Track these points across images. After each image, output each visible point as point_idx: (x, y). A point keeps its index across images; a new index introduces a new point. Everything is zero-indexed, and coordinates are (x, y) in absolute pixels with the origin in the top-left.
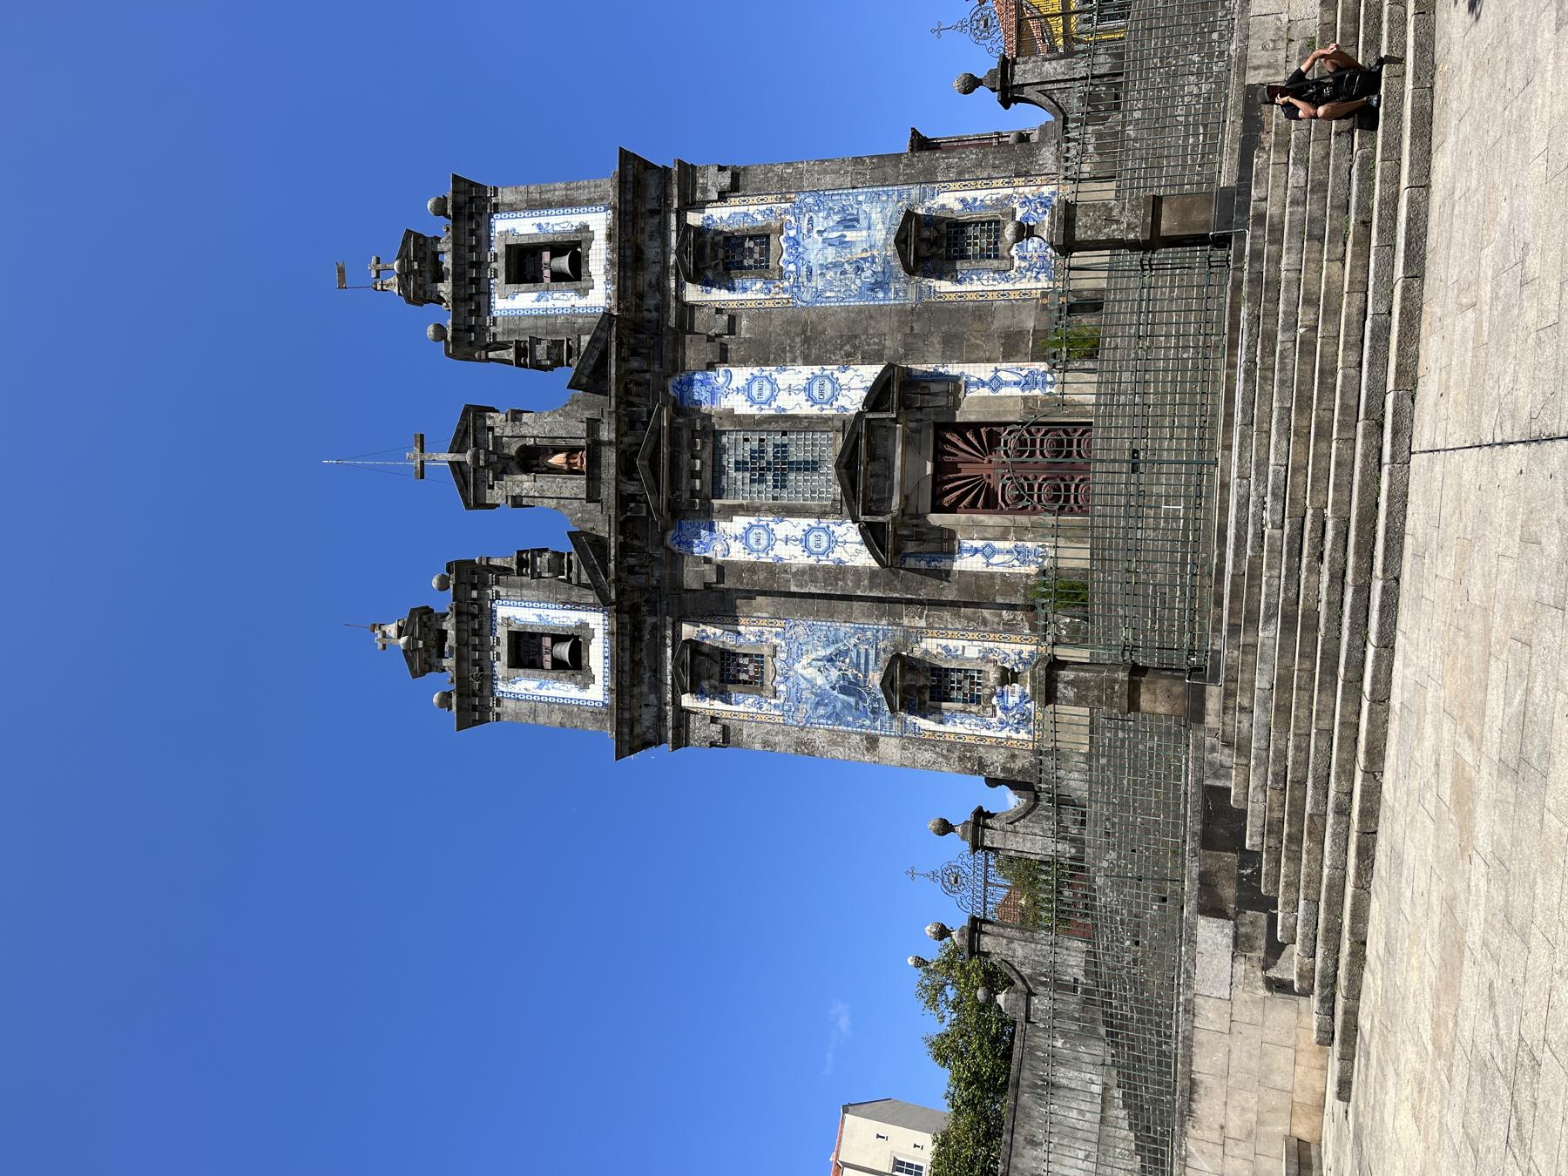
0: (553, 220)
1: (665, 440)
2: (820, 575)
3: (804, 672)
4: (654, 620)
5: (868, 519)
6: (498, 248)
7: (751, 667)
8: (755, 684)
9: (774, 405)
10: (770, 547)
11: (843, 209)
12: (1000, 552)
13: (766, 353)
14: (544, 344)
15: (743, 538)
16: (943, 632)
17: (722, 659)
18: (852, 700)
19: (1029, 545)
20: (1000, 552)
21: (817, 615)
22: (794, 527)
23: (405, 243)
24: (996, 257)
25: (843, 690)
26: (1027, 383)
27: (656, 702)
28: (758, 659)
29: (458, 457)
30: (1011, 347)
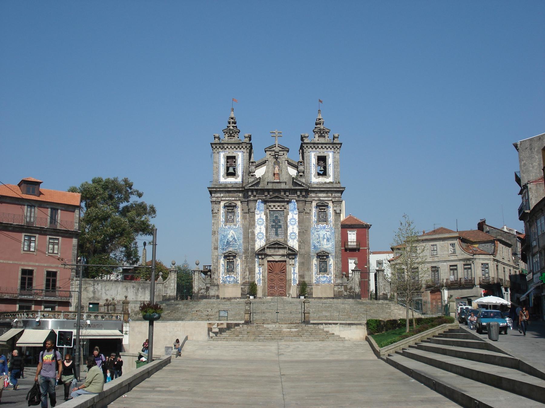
0: (331, 168)
1: (282, 200)
2: (253, 236)
3: (231, 232)
4: (241, 196)
5: (266, 248)
6: (325, 154)
7: (231, 219)
8: (227, 221)
9: (290, 225)
10: (259, 224)
11: (331, 239)
12: (260, 276)
13: (301, 222)
14: (303, 169)
15: (260, 218)
16: (242, 264)
17: (232, 212)
18: (225, 244)
19: (261, 282)
20: (260, 276)
21: (244, 235)
22: (263, 230)
23: (327, 129)
24: (320, 272)
25: (227, 241)
26: (294, 280)
27: (221, 196)
28: (233, 221)
29: (277, 146)
30: (301, 276)
